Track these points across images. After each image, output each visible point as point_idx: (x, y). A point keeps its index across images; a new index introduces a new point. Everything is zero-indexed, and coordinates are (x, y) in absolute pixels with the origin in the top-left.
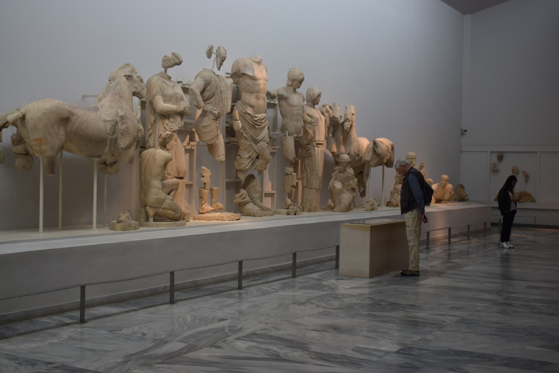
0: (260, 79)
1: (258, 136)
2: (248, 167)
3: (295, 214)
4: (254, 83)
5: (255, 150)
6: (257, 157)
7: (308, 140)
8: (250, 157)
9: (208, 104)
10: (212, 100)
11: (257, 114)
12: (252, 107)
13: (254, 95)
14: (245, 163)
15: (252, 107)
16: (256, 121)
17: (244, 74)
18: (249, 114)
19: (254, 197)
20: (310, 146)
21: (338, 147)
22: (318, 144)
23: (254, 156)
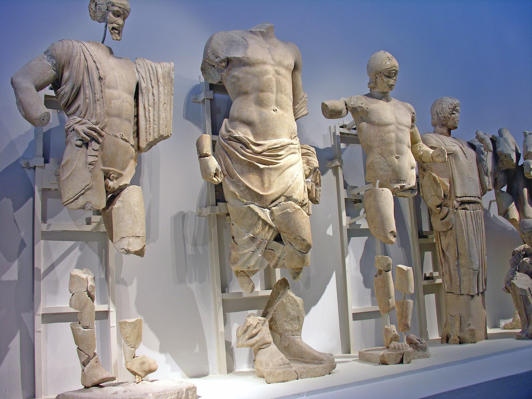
0: (264, 63)
1: (269, 188)
2: (252, 263)
3: (401, 362)
4: (248, 73)
5: (265, 223)
6: (278, 239)
7: (439, 197)
8: (253, 239)
9: (74, 113)
10: (80, 101)
11: (266, 140)
12: (249, 123)
13: (252, 97)
14: (244, 254)
15: (249, 123)
16: (260, 154)
17: (228, 61)
18: (238, 140)
19: (286, 331)
20: (445, 210)
21: (521, 209)
22: (463, 203)
23: (269, 235)
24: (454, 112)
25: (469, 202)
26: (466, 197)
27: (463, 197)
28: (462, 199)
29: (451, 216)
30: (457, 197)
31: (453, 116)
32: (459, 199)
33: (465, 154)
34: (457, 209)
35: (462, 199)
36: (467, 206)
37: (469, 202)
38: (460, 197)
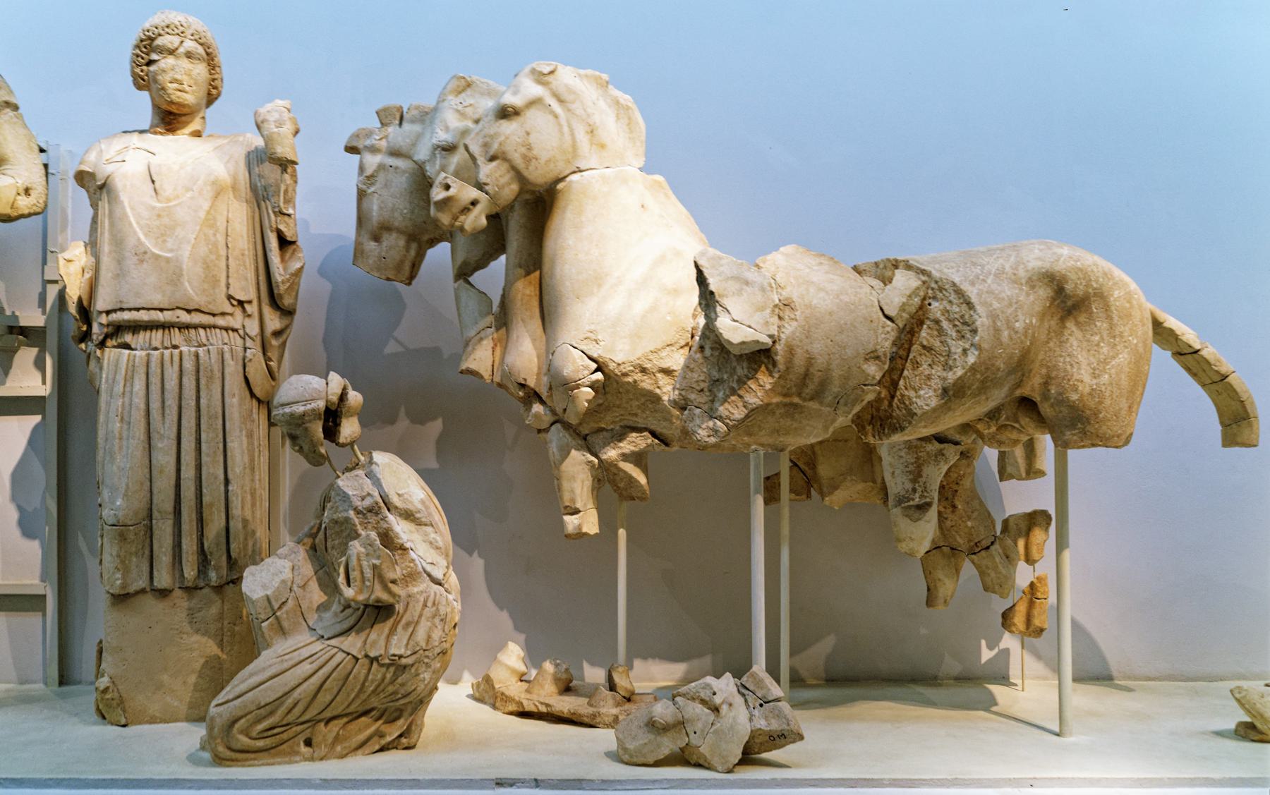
22: (117, 329)
24: (154, 56)
25: (136, 327)
26: (122, 309)
27: (115, 311)
28: (114, 317)
29: (93, 364)
30: (101, 313)
31: (152, 68)
32: (104, 319)
33: (153, 182)
34: (102, 345)
35: (114, 317)
36: (128, 338)
37: (136, 327)
38: (108, 313)
